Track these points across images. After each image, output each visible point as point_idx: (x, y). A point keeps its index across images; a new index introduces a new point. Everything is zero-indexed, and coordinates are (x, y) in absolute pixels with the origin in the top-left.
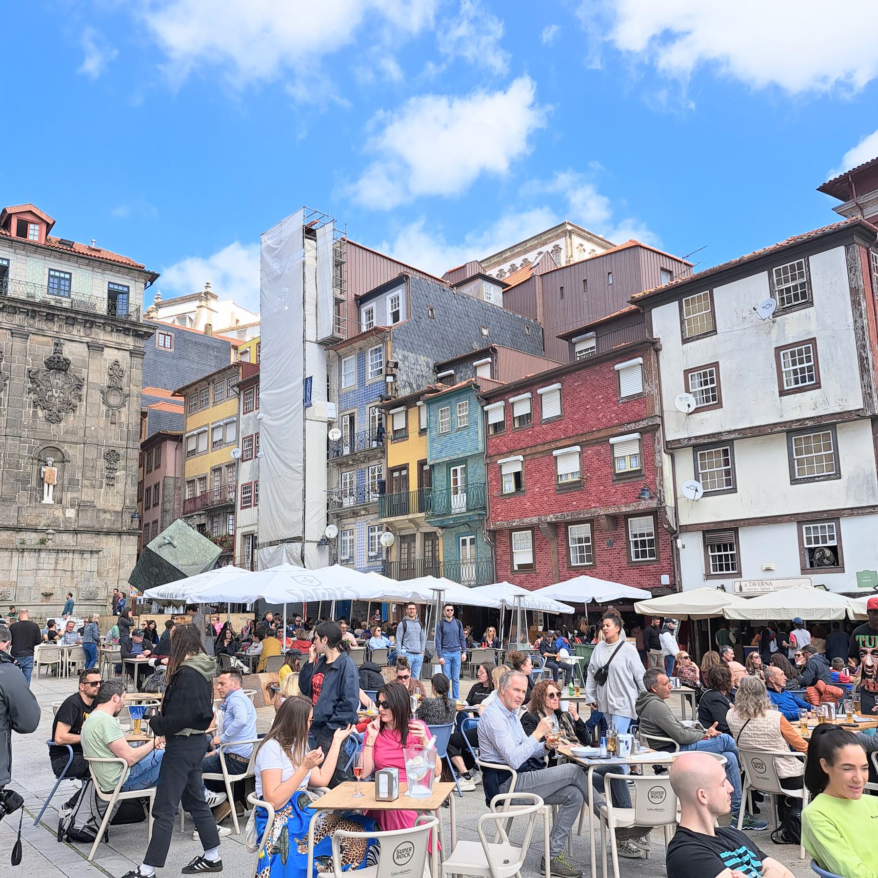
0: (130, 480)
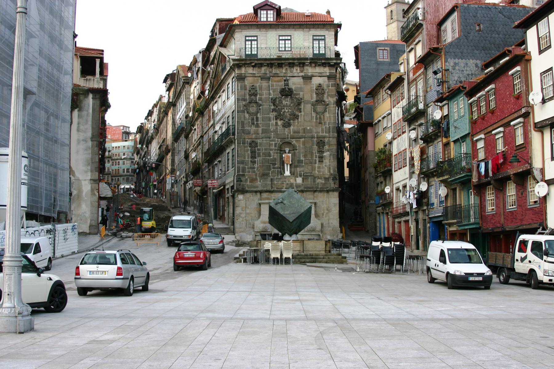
0: (332, 157)
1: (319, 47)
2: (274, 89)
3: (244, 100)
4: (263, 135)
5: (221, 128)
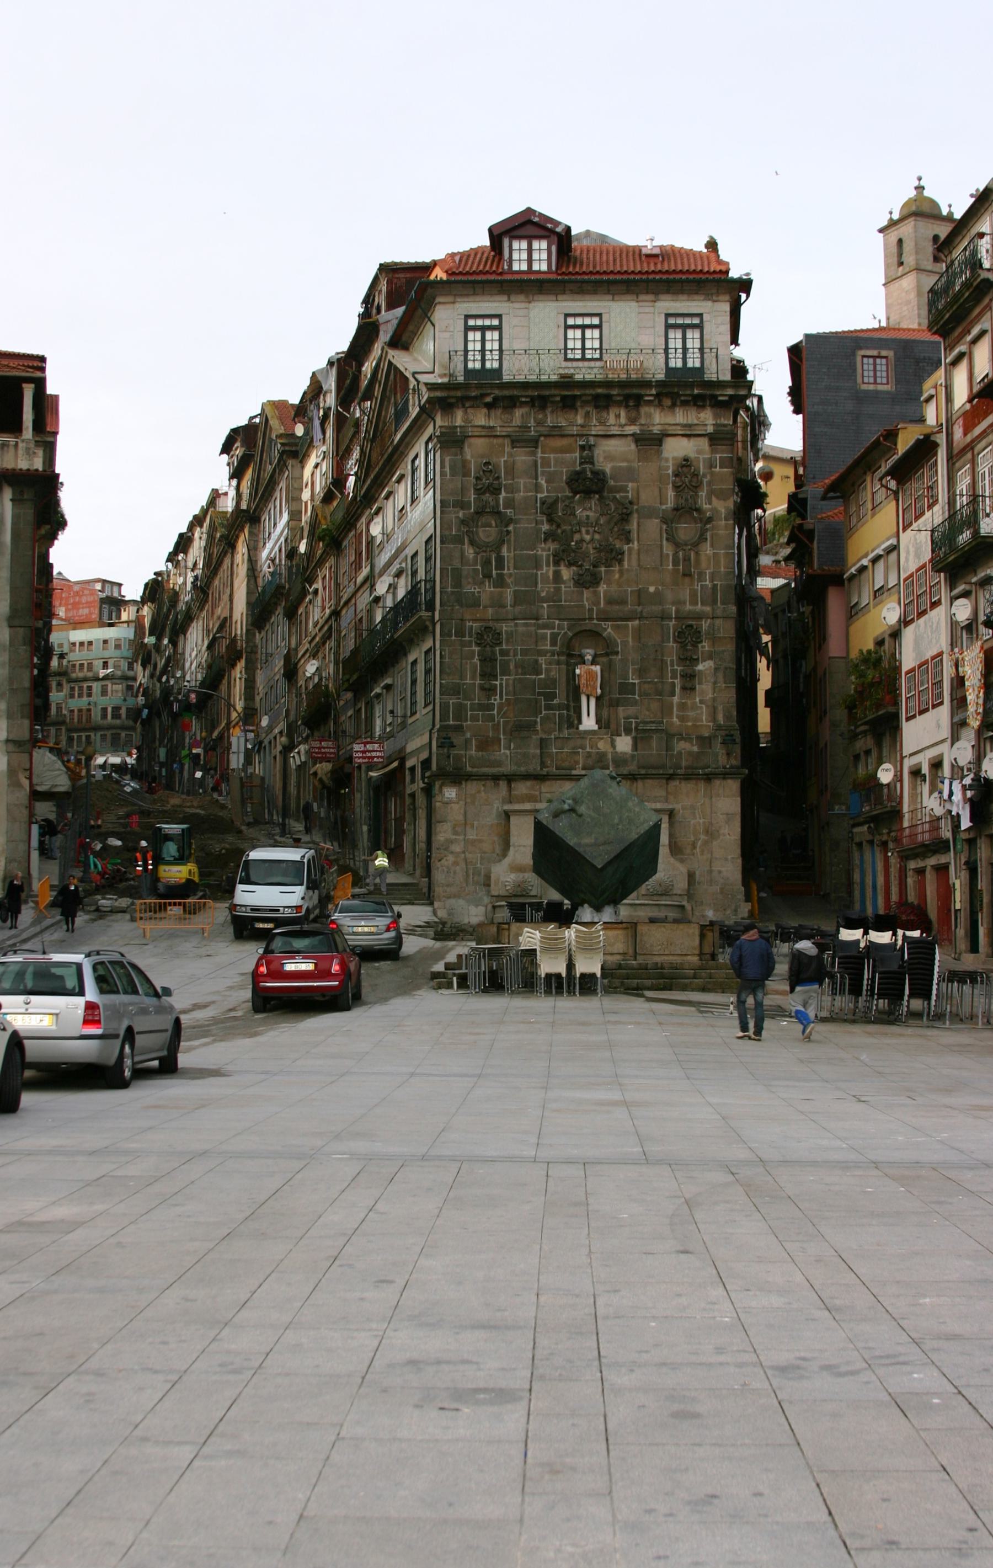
0: (721, 678)
1: (685, 349)
2: (549, 472)
3: (462, 505)
4: (518, 608)
5: (392, 587)
